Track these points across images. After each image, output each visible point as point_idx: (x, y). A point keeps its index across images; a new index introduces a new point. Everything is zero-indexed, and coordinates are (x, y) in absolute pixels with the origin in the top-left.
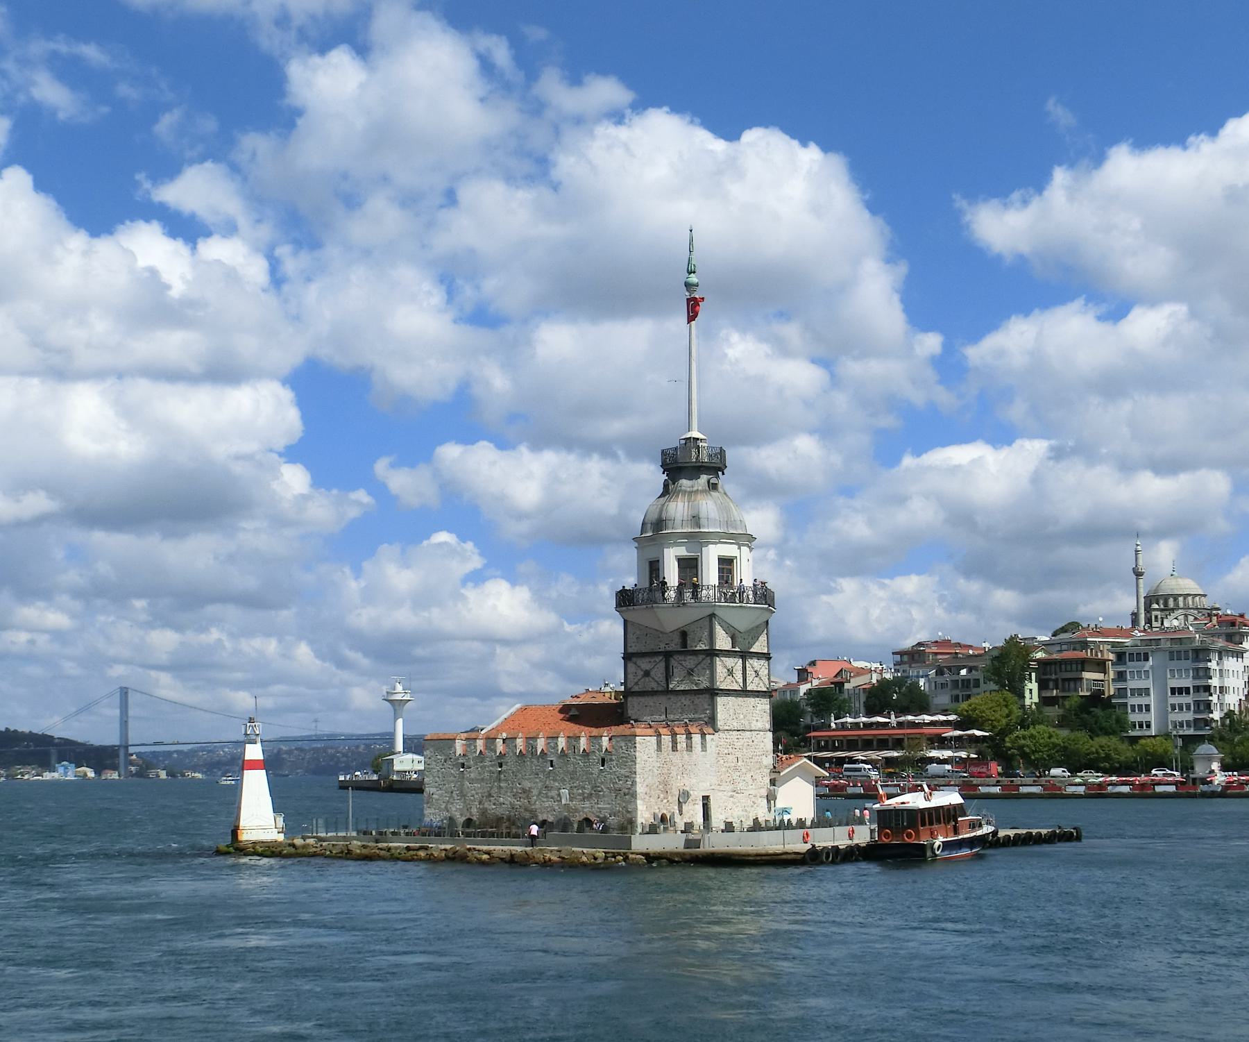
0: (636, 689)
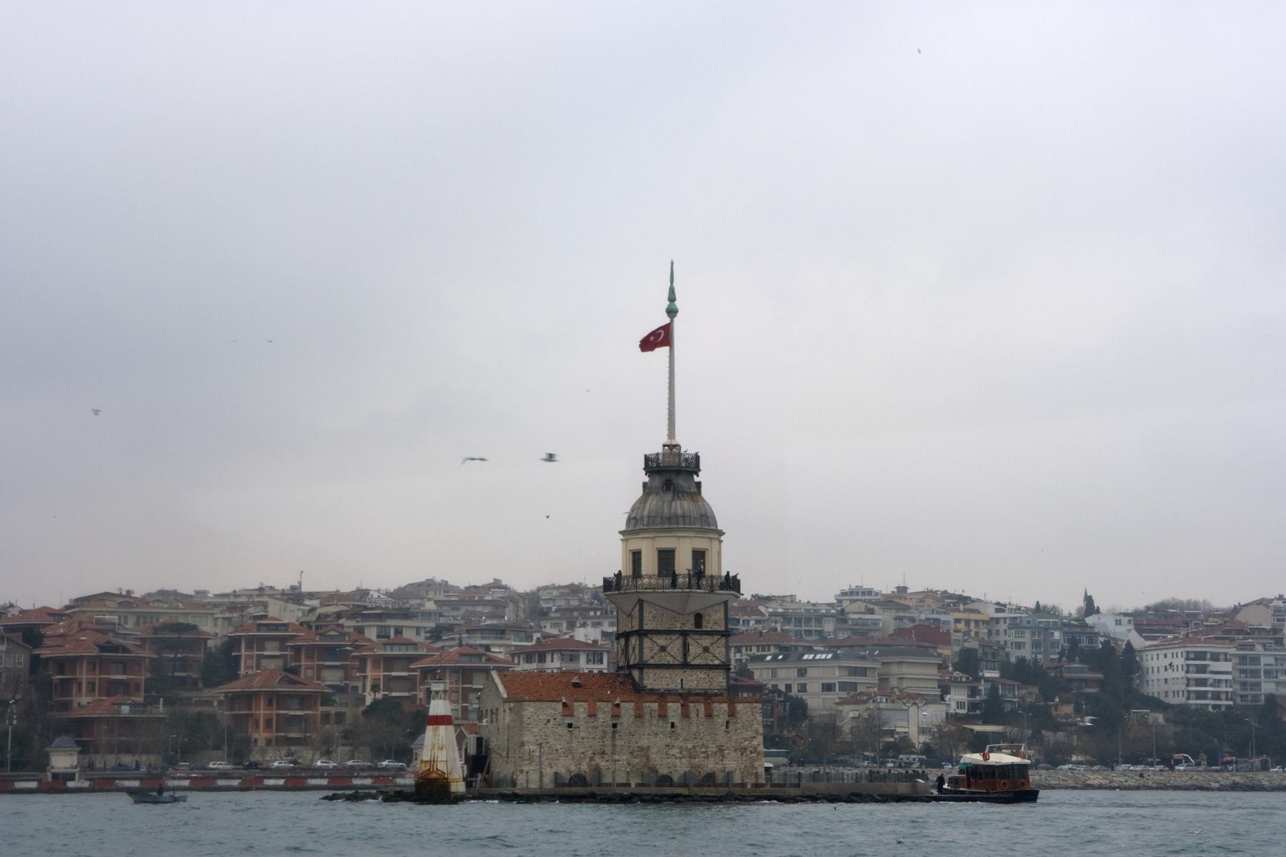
0: (652, 662)
